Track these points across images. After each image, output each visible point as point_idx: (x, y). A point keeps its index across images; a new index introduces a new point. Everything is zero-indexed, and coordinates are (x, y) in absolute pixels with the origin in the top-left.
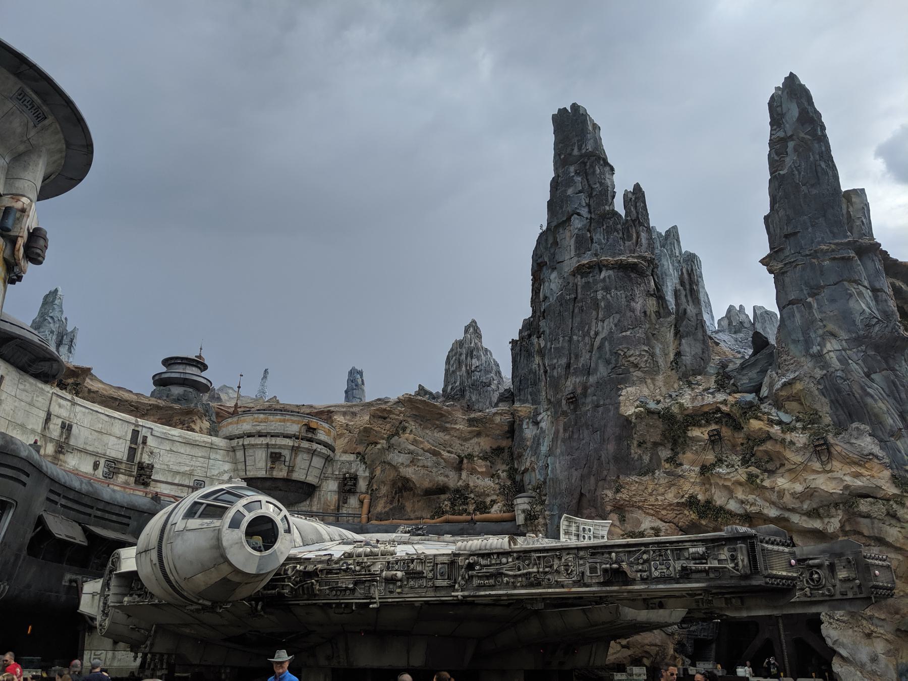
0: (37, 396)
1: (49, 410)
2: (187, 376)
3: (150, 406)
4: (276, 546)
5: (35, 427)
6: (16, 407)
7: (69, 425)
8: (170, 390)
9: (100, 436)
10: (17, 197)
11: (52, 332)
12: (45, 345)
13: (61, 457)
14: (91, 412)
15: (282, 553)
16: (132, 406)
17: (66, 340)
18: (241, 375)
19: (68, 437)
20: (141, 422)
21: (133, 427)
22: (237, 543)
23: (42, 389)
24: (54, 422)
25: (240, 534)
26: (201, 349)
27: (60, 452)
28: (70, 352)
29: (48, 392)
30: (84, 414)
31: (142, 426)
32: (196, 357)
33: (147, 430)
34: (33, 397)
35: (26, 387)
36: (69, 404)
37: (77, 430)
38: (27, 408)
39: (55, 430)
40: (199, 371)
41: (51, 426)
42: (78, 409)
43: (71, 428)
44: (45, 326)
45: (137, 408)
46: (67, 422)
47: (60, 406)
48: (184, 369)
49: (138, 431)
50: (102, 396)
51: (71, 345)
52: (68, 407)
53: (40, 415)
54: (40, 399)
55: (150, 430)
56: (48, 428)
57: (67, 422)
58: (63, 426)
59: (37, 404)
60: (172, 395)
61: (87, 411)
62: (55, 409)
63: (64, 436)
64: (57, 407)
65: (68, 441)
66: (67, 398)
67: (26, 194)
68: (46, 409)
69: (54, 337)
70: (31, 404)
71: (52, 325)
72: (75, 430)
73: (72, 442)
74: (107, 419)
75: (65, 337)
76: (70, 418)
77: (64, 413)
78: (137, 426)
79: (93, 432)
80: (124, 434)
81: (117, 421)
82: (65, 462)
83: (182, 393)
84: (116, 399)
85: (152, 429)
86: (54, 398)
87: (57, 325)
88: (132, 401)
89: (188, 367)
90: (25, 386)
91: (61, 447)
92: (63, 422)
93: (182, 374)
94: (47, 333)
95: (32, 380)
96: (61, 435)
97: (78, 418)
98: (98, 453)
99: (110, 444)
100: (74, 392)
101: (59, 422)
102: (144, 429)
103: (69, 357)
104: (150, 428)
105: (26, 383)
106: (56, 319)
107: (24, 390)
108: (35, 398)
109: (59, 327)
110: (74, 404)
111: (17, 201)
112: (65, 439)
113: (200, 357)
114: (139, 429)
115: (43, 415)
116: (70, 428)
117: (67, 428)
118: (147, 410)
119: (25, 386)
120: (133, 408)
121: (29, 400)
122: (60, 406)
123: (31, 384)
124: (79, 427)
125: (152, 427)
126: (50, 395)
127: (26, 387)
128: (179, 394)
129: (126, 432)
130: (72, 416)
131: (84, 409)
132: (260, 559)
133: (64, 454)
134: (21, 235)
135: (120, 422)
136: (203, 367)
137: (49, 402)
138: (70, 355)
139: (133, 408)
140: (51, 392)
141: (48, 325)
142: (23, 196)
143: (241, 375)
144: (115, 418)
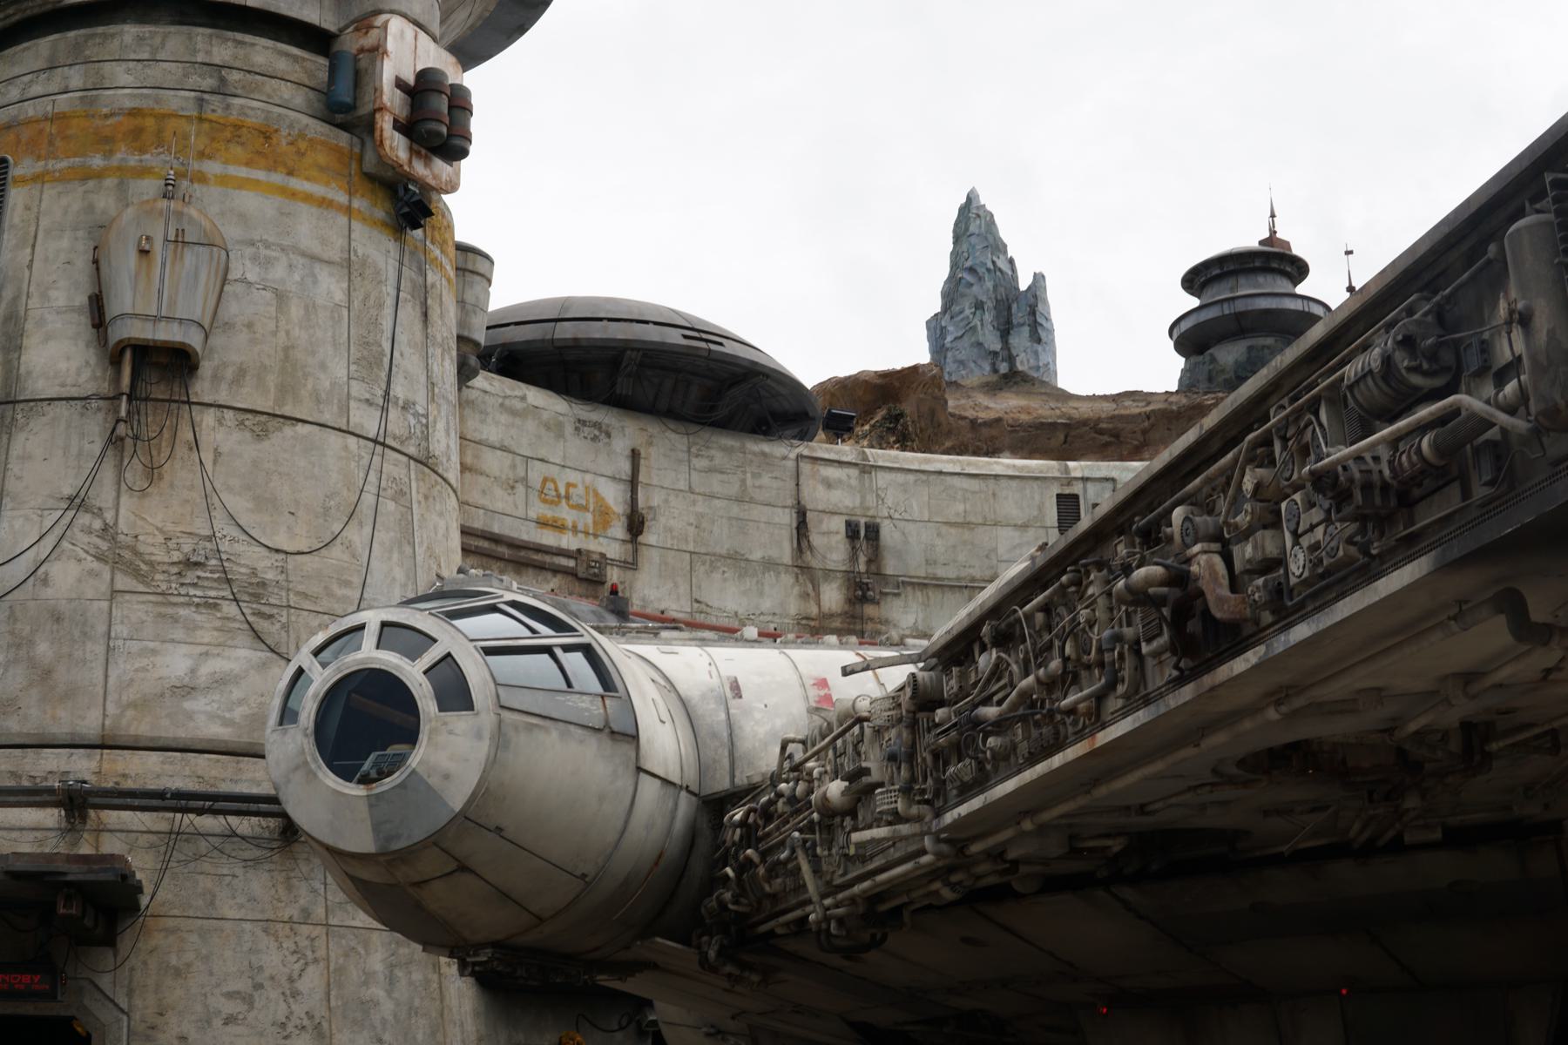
0: (756, 476)
1: (799, 503)
2: (1240, 306)
3: (1148, 417)
4: (416, 759)
5: (773, 553)
6: (700, 516)
7: (867, 526)
8: (1213, 360)
9: (967, 535)
10: (366, 22)
11: (979, 306)
12: (703, 345)
13: (870, 610)
14: (924, 477)
15: (447, 777)
16: (1101, 432)
17: (1019, 315)
18: (1349, 253)
19: (875, 558)
20: (1077, 467)
21: (1056, 489)
22: (297, 768)
23: (764, 454)
24: (824, 527)
25: (300, 738)
26: (1273, 216)
27: (864, 599)
28: (1039, 341)
29: (785, 458)
30: (904, 488)
31: (1085, 480)
32: (1261, 243)
33: (1098, 486)
34: (743, 481)
35: (717, 462)
36: (854, 472)
37: (897, 535)
38: (735, 510)
39: (831, 546)
40: (1290, 286)
41: (816, 539)
42: (882, 479)
43: (877, 532)
44: (963, 295)
45: (1117, 436)
46: (863, 521)
47: (828, 484)
48: (1232, 290)
49: (1076, 497)
50: (1016, 427)
51: (1035, 321)
52: (854, 482)
53: (777, 520)
54: (765, 480)
55: (1109, 485)
56: (810, 547)
57: (863, 521)
58: (852, 531)
59: (759, 495)
60: (1223, 371)
61: (911, 477)
62: (816, 495)
63: (862, 559)
64: (821, 488)
65: (879, 568)
66: (845, 459)
67: (381, 7)
68: (790, 502)
69: (988, 317)
70: (741, 499)
71: (975, 289)
72: (888, 533)
73: (891, 567)
74: (974, 485)
75: (1014, 306)
76: (868, 509)
77: (844, 499)
78: (1070, 481)
79: (944, 529)
80: (1035, 513)
81: (1004, 482)
82: (887, 622)
83: (1243, 358)
84: (1054, 426)
85: (1113, 480)
86: (806, 467)
87: (989, 284)
88: (1099, 420)
89: (1242, 280)
90: (711, 458)
91: (864, 587)
92: (848, 524)
93: (1226, 306)
94: (968, 312)
95: (728, 441)
96: (853, 558)
97: (889, 502)
98: (973, 580)
99: (1001, 551)
100: (892, 439)
101: (838, 524)
102: (1089, 485)
103: (1036, 353)
104: (1107, 479)
105: (713, 452)
106: (981, 270)
107: (711, 470)
108: (749, 482)
109: (995, 287)
110: (866, 469)
111: (367, 33)
112: (869, 562)
113: (1272, 239)
114: (1077, 489)
115: (787, 518)
116: (873, 531)
117: (863, 535)
118: (1144, 432)
119: (711, 458)
120: (1106, 438)
121: (734, 489)
122: (828, 484)
123: (728, 450)
124: (901, 524)
125: (1114, 474)
126: (791, 464)
127: (717, 462)
128: (1236, 362)
129: (1040, 508)
130: (871, 500)
131: (900, 477)
132: (371, 806)
133: (878, 603)
134: (377, 106)
135: (1014, 483)
136: (1299, 269)
137: (793, 484)
138: (1040, 348)
139: (1106, 438)
140: (793, 455)
141: (968, 291)
142: (379, 12)
143: (1349, 253)
144: (996, 477)
